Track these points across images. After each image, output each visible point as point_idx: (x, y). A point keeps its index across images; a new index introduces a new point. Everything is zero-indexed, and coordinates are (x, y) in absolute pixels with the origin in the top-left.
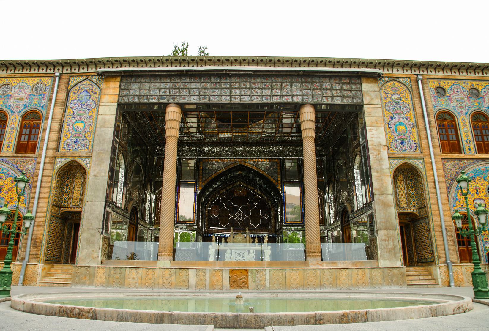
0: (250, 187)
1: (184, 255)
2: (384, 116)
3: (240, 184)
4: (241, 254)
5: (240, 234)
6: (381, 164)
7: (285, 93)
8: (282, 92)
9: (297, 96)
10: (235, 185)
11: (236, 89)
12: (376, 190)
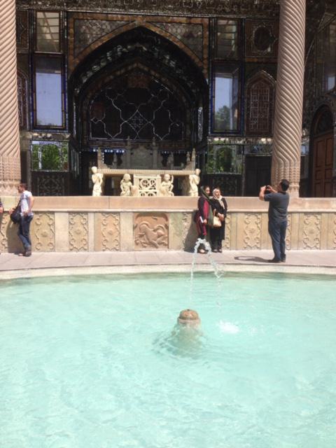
0: (153, 73)
1: (51, 182)
3: (137, 67)
4: (149, 182)
10: (130, 68)
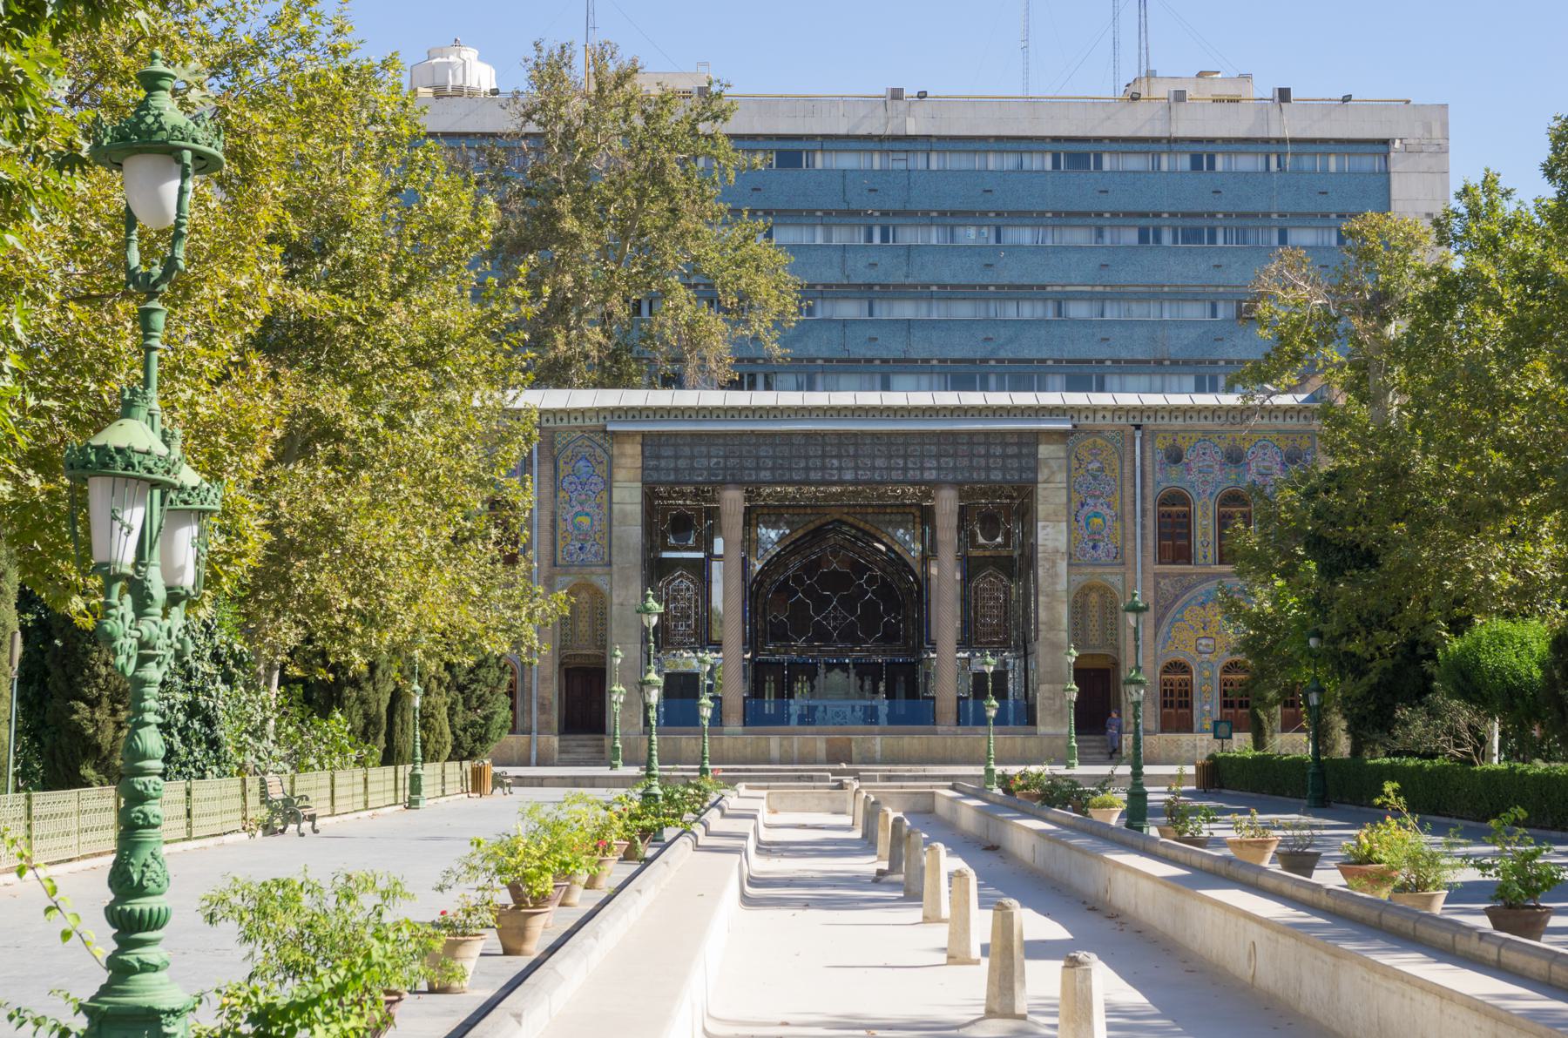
2: (1069, 500)
5: (837, 670)
6: (1054, 583)
7: (910, 465)
8: (906, 463)
9: (930, 469)
11: (832, 457)
12: (1044, 623)
